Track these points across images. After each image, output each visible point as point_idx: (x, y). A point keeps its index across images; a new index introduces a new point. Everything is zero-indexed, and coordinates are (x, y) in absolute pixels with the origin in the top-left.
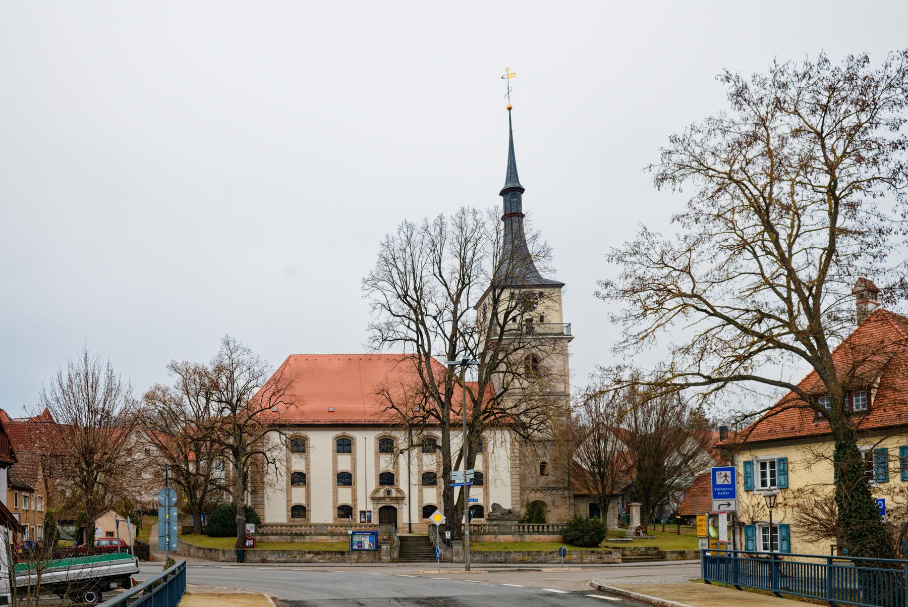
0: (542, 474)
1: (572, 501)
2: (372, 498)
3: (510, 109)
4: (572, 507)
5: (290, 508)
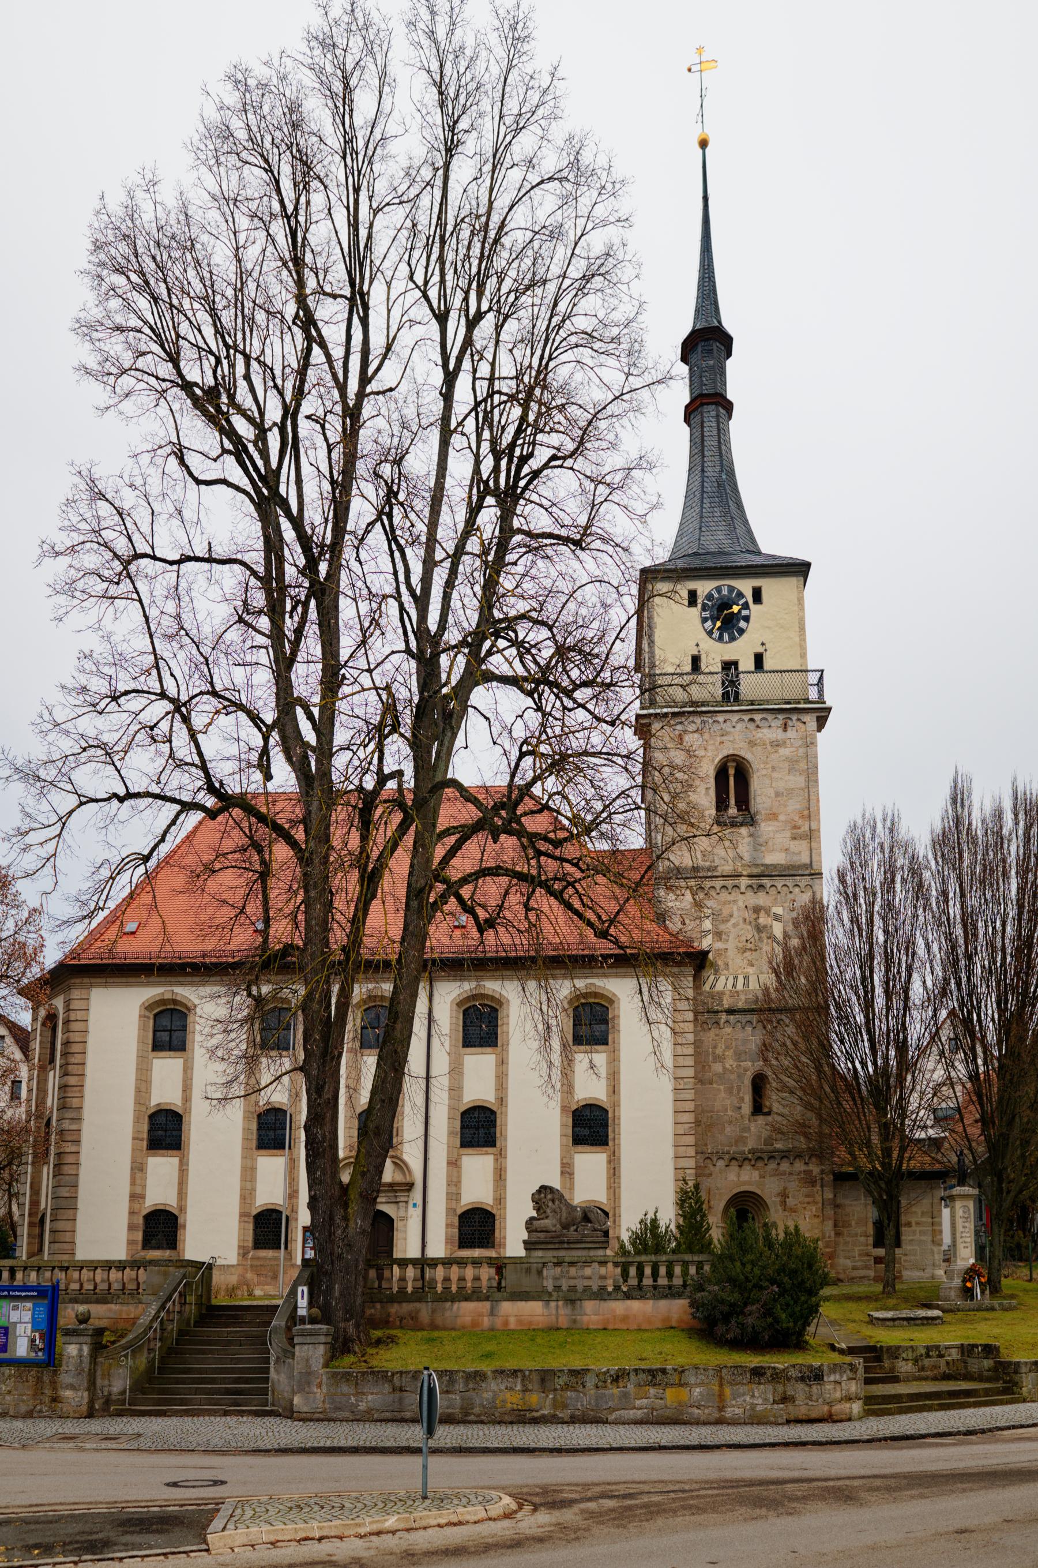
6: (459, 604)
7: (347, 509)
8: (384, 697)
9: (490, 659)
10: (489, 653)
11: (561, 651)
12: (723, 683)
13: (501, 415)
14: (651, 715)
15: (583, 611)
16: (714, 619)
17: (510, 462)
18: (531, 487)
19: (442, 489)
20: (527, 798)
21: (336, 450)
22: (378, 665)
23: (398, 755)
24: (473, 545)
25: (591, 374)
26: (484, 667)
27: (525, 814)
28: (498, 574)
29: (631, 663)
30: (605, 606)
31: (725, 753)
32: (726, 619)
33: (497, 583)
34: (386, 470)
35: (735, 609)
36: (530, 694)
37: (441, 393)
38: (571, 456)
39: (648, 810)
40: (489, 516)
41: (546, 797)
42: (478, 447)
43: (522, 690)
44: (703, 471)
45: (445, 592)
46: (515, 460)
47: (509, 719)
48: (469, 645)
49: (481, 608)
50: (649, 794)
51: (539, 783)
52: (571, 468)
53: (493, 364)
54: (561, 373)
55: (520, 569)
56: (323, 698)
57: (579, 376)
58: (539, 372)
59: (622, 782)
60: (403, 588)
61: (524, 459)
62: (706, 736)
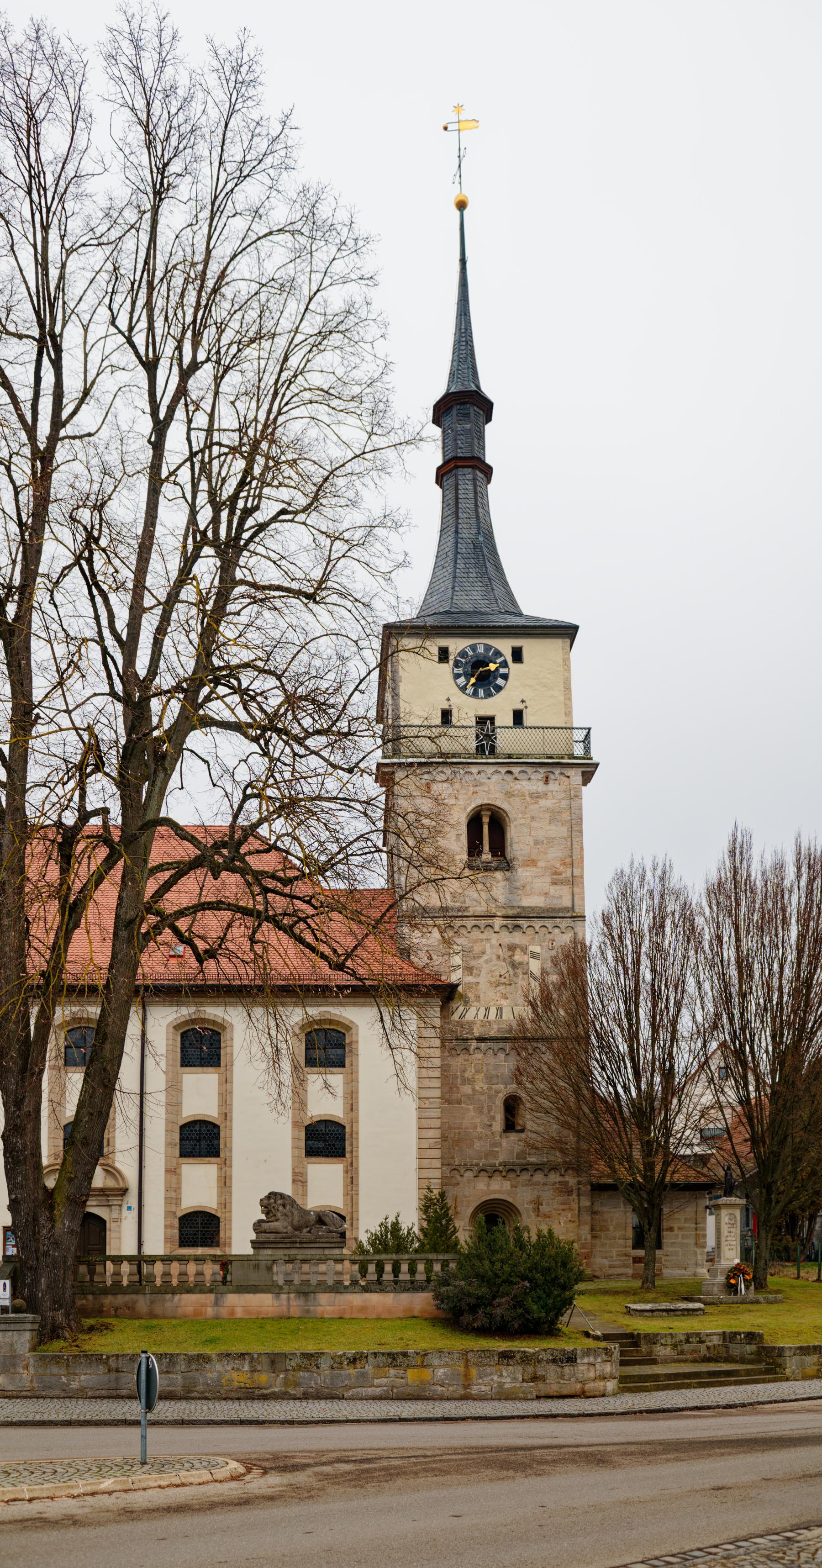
0: (510, 1126)
1: (586, 1202)
3: (461, 206)
4: (586, 1218)
6: (172, 651)
7: (39, 552)
8: (86, 737)
9: (209, 705)
10: (208, 699)
11: (291, 701)
12: (477, 737)
13: (221, 467)
14: (394, 764)
15: (317, 662)
16: (468, 676)
17: (232, 513)
18: (257, 539)
19: (152, 537)
20: (251, 838)
21: (25, 492)
22: (78, 706)
23: (103, 792)
24: (188, 593)
25: (328, 431)
26: (201, 712)
27: (250, 853)
28: (218, 622)
29: (372, 714)
30: (343, 659)
31: (479, 802)
32: (482, 676)
33: (217, 631)
34: (85, 515)
35: (492, 667)
36: (256, 740)
37: (149, 442)
38: (303, 511)
39: (390, 853)
40: (207, 567)
41: (274, 838)
42: (194, 497)
43: (246, 736)
44: (457, 532)
45: (155, 638)
46: (238, 512)
47: (231, 763)
48: (184, 691)
49: (199, 656)
50: (392, 839)
51: (266, 825)
52: (304, 523)
53: (211, 416)
54: (292, 428)
55: (244, 619)
56: (13, 735)
57: (313, 432)
58: (266, 426)
59: (361, 826)
60: (106, 633)
61: (248, 512)
62: (457, 786)
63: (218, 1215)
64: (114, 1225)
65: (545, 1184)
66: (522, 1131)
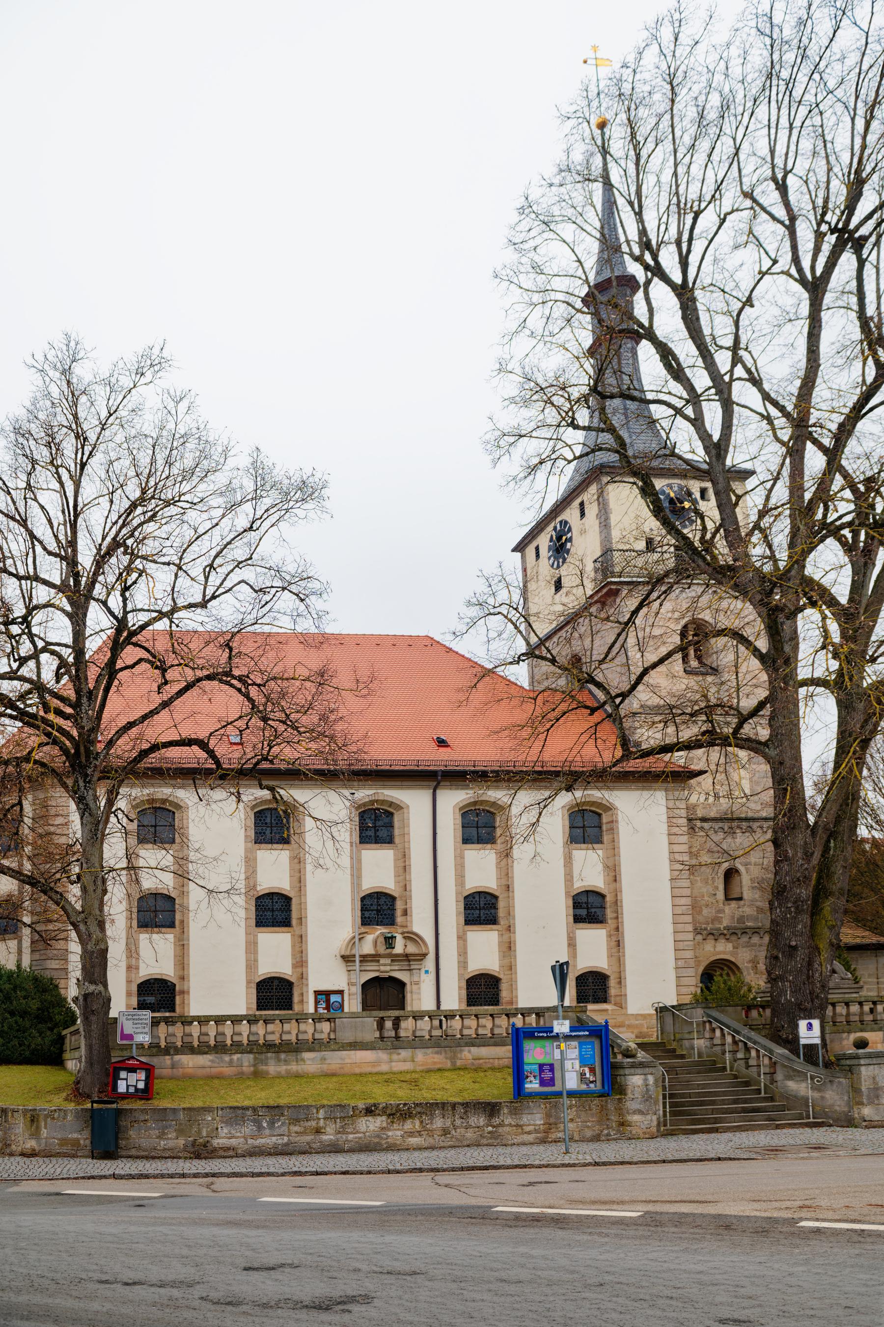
2: (347, 959)
5: (135, 988)
63: (501, 976)
64: (414, 987)
65: (760, 945)
66: (741, 899)
